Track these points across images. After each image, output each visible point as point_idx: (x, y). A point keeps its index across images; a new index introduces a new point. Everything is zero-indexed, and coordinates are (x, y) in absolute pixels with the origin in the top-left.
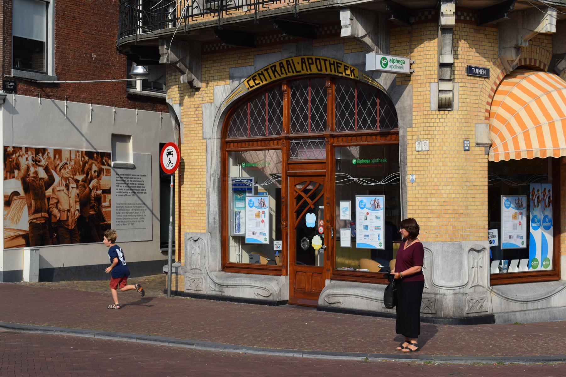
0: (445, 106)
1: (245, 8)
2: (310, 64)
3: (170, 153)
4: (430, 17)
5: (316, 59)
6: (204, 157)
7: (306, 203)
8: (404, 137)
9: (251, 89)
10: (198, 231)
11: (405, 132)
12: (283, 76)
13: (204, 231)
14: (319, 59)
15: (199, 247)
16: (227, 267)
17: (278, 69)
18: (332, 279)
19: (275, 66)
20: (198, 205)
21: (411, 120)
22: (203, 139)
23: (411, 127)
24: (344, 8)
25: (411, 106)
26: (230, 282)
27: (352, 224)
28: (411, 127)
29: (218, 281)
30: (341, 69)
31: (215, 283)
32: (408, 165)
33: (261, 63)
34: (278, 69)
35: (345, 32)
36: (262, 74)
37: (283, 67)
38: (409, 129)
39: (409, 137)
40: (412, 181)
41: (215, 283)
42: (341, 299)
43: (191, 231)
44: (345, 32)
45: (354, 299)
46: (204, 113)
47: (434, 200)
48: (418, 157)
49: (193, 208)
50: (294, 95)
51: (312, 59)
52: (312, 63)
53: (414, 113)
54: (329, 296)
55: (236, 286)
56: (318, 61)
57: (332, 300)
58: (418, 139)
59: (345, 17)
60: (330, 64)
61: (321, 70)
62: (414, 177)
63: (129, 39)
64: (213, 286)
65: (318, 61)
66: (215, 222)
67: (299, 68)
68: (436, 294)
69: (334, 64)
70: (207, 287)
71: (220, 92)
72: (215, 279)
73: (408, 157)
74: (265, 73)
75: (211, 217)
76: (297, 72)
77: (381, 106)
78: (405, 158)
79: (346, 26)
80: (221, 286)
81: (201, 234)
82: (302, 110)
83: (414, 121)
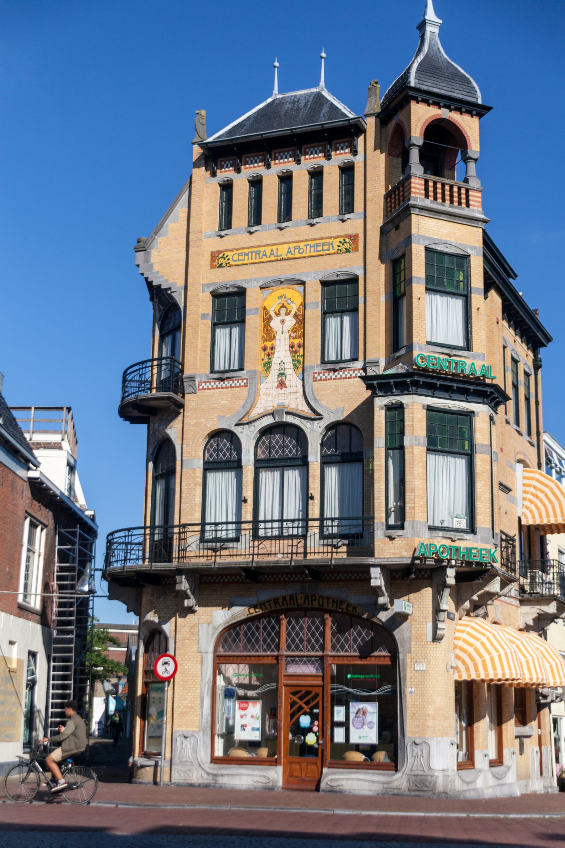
1: (280, 556)
2: (312, 600)
3: (166, 663)
4: (426, 576)
5: (320, 597)
6: (199, 667)
7: (300, 708)
8: (404, 660)
9: (250, 616)
10: (189, 729)
11: (405, 656)
12: (283, 607)
13: (197, 729)
14: (323, 597)
15: (190, 743)
16: (215, 760)
17: (280, 601)
18: (329, 767)
19: (278, 599)
20: (191, 708)
21: (410, 648)
22: (199, 652)
23: (410, 652)
24: (374, 566)
25: (410, 639)
26: (220, 772)
27: (346, 725)
28: (410, 652)
29: (211, 771)
30: (344, 606)
31: (208, 774)
32: (408, 680)
33: (264, 596)
34: (280, 601)
35: (373, 583)
36: (264, 604)
37: (286, 600)
38: (408, 655)
39: (408, 660)
40: (411, 692)
41: (208, 774)
42: (344, 783)
43: (182, 729)
44: (373, 583)
45: (356, 782)
46: (201, 632)
47: (430, 706)
48: (417, 675)
49: (185, 710)
50: (289, 623)
51: (315, 597)
52: (315, 600)
53: (413, 643)
54: (331, 780)
55: (232, 775)
56: (321, 599)
57: (334, 784)
58: (416, 662)
59: (375, 572)
60: (333, 601)
61: (323, 605)
62: (413, 690)
64: (205, 776)
65: (321, 599)
66: (207, 723)
67: (301, 602)
68: (432, 776)
69: (337, 602)
70: (197, 777)
71: (220, 617)
72: (208, 770)
73: (408, 675)
74: (267, 604)
75: (204, 717)
76: (298, 605)
77: (385, 635)
78: (405, 675)
79: (376, 578)
80: (215, 775)
81: (193, 732)
82: (297, 634)
83: (413, 649)
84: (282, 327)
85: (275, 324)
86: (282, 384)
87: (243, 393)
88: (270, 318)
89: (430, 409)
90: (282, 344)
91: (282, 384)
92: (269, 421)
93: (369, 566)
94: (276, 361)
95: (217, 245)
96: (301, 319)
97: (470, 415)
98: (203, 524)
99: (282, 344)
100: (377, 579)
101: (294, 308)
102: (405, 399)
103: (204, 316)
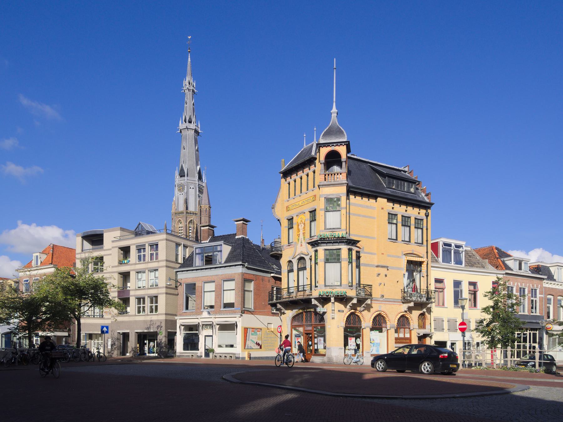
0: (333, 318)
35: (313, 303)
59: (313, 300)
63: (271, 302)
84: (301, 227)
85: (300, 227)
86: (301, 245)
87: (293, 249)
88: (298, 226)
89: (326, 250)
90: (301, 232)
91: (301, 245)
92: (298, 257)
93: (311, 299)
94: (300, 238)
95: (286, 204)
96: (304, 224)
97: (340, 249)
98: (288, 288)
99: (301, 232)
100: (314, 302)
101: (303, 221)
102: (318, 248)
103: (285, 227)
